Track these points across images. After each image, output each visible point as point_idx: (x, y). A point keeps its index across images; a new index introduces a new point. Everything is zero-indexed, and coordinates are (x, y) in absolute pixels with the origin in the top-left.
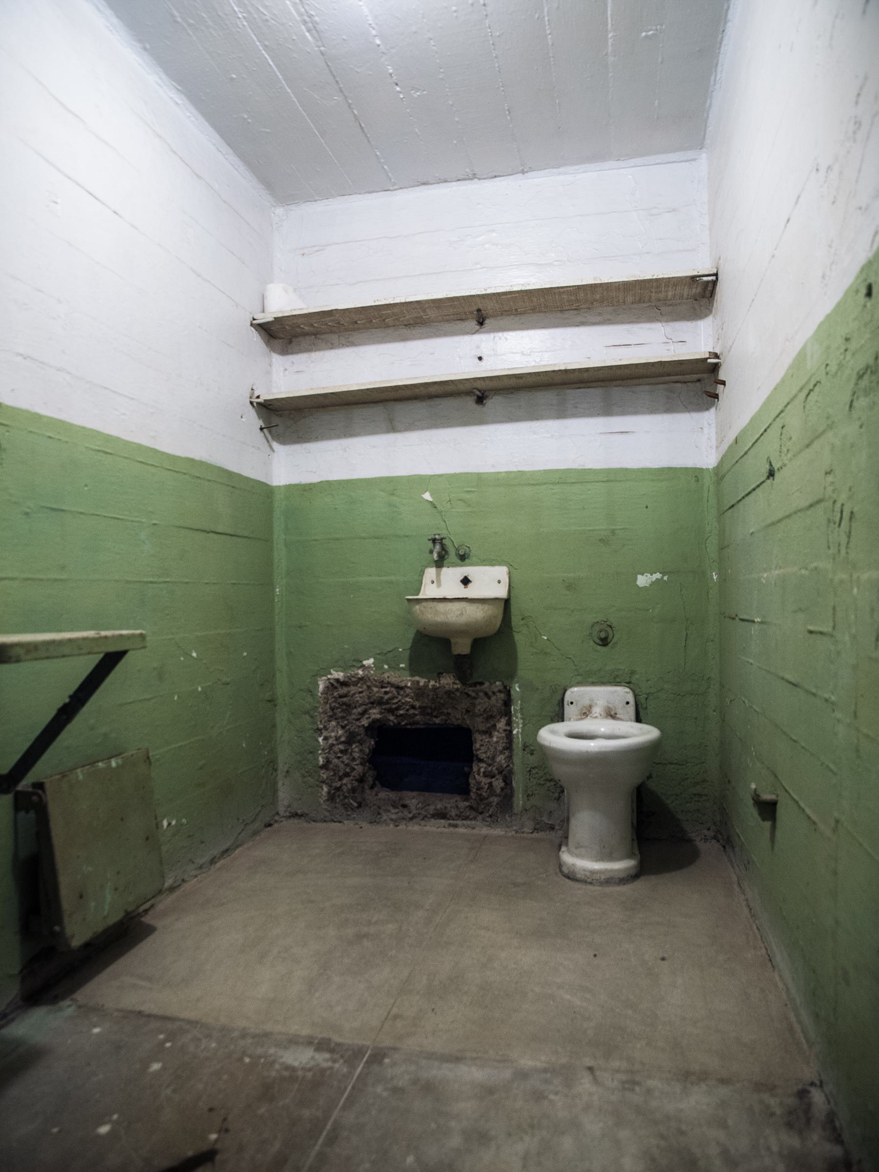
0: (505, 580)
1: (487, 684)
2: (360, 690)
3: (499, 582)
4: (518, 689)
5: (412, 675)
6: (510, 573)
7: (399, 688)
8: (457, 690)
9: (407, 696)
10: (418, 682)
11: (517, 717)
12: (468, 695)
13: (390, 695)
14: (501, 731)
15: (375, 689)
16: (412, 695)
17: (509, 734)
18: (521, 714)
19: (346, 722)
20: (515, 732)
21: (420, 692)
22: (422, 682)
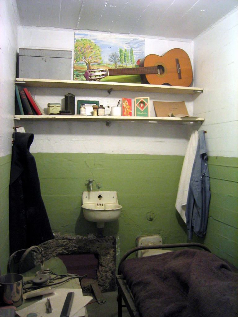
0: (115, 196)
1: (107, 237)
2: (53, 241)
3: (113, 197)
4: (119, 238)
5: (76, 235)
6: (117, 194)
7: (70, 240)
8: (95, 240)
9: (73, 243)
10: (79, 237)
11: (118, 249)
12: (98, 241)
13: (66, 243)
14: (111, 254)
15: (60, 241)
16: (76, 242)
17: (115, 257)
18: (120, 248)
19: (45, 255)
20: (117, 255)
21: (79, 241)
22: (80, 237)
